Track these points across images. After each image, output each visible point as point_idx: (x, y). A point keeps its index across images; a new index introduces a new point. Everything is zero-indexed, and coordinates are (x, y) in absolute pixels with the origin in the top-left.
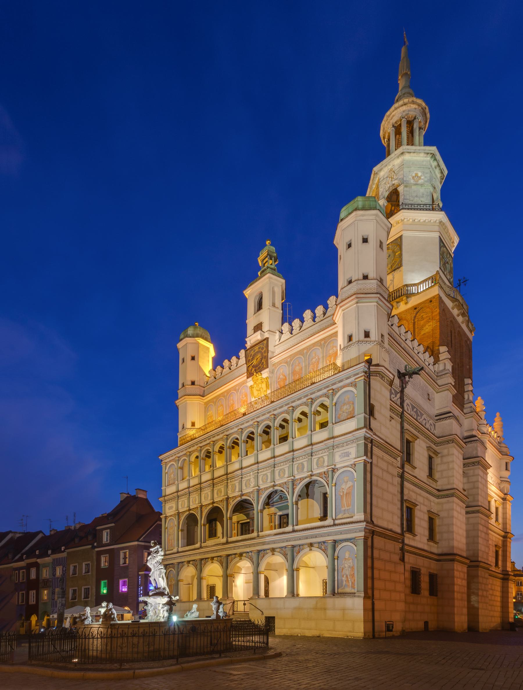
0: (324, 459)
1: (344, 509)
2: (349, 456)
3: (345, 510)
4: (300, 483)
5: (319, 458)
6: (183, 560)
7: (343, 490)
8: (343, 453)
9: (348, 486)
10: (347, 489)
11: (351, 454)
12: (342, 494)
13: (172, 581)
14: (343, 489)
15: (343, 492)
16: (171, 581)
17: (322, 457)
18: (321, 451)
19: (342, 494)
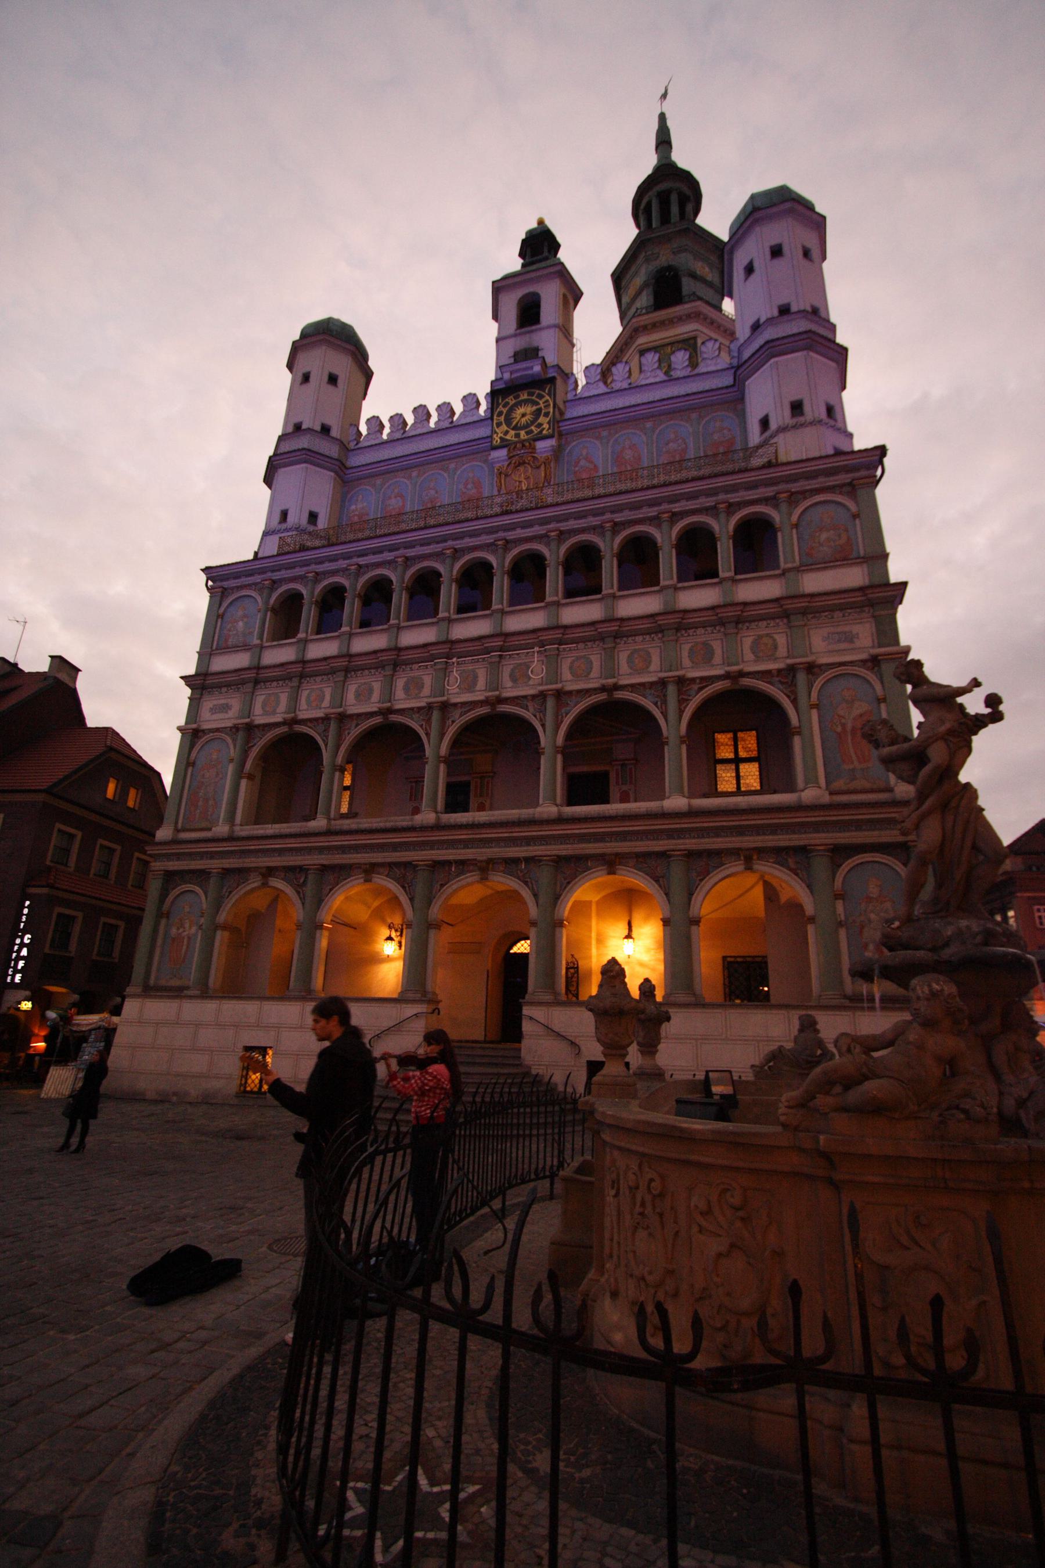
0: (774, 640)
1: (851, 767)
2: (851, 641)
3: (853, 770)
4: (701, 689)
5: (760, 637)
6: (250, 862)
7: (843, 721)
8: (833, 633)
9: (856, 712)
10: (854, 719)
11: (858, 638)
12: (839, 729)
13: (187, 925)
14: (843, 717)
15: (844, 726)
16: (182, 926)
17: (767, 635)
18: (765, 623)
19: (839, 729)
